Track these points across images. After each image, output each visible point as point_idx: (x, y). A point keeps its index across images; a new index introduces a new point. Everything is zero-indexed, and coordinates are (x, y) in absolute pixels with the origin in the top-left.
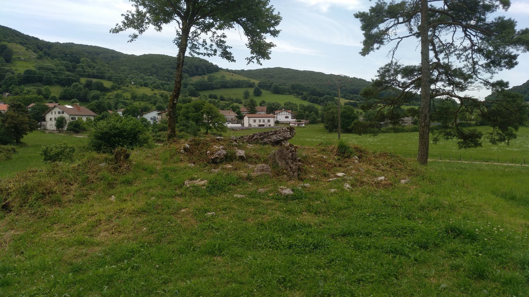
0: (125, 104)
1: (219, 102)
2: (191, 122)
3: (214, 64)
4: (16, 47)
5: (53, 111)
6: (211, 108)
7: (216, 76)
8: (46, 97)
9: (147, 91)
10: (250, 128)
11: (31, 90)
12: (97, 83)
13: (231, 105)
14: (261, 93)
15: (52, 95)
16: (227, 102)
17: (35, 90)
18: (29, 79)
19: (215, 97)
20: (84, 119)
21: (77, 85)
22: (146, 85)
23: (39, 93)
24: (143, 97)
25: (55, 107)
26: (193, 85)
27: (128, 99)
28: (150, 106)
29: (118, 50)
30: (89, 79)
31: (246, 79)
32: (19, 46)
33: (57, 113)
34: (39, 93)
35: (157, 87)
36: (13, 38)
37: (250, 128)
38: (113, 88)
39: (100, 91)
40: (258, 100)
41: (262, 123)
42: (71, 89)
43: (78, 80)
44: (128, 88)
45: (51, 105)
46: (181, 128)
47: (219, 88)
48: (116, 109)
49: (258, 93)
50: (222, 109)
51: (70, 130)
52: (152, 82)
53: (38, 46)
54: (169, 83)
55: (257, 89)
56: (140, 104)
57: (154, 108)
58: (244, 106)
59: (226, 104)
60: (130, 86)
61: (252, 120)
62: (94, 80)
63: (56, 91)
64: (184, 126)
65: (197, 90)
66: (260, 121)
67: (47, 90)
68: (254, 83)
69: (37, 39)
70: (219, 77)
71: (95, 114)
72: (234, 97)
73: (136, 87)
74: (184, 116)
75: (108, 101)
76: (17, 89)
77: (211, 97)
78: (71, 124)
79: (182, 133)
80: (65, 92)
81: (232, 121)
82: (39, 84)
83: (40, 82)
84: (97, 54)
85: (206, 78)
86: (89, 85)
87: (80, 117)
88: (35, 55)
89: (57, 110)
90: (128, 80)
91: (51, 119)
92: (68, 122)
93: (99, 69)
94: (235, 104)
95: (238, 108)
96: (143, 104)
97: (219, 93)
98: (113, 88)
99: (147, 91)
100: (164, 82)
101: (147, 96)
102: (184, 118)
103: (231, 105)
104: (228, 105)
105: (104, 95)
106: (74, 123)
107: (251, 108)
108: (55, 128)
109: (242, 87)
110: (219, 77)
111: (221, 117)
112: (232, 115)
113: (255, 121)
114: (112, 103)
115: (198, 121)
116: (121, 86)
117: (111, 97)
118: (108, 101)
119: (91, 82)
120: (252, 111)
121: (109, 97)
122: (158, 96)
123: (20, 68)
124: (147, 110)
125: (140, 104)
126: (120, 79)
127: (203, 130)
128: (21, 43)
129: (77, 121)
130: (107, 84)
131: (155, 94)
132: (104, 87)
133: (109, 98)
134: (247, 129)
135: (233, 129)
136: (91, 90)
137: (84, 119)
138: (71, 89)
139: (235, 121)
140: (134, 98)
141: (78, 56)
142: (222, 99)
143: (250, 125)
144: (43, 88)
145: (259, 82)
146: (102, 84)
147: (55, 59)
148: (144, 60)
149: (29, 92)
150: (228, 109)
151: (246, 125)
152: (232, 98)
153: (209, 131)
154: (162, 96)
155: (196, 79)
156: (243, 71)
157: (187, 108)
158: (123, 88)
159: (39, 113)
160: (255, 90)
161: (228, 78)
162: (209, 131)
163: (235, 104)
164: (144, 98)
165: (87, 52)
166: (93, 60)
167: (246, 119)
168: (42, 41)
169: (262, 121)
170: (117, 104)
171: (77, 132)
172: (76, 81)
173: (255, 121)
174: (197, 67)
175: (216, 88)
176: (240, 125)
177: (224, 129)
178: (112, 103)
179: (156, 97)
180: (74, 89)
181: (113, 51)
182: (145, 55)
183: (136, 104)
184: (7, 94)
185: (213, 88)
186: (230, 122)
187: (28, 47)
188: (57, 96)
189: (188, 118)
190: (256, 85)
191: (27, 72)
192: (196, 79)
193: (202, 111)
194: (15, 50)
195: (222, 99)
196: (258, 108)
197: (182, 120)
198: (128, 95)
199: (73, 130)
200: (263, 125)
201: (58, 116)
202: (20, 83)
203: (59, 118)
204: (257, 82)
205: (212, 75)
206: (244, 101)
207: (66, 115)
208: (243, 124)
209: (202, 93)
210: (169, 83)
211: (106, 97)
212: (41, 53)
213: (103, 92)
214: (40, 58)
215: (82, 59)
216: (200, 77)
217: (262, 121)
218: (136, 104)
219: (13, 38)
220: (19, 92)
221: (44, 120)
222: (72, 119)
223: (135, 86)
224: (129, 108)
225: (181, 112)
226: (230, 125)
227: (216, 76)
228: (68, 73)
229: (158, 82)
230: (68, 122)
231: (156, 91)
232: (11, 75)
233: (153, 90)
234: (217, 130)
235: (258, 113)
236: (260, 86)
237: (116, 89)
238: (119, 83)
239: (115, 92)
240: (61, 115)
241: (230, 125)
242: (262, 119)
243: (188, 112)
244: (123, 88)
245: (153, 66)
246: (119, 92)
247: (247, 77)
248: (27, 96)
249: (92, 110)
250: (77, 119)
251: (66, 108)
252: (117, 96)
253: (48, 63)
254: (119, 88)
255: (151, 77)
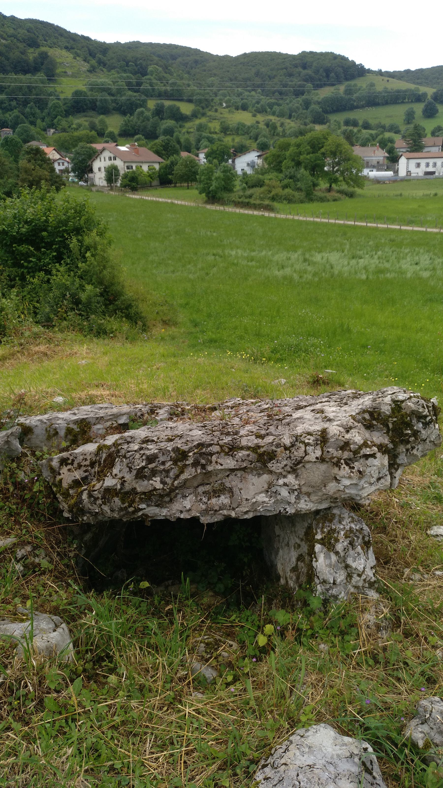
0: (211, 141)
1: (359, 131)
2: (302, 170)
3: (357, 63)
4: (61, 55)
5: (102, 156)
6: (338, 146)
7: (359, 85)
8: (101, 134)
9: (245, 118)
10: (408, 179)
11: (81, 122)
12: (171, 108)
13: (380, 137)
14: (437, 111)
15: (110, 129)
16: (373, 132)
17: (87, 124)
18: (79, 105)
19: (355, 124)
20: (145, 168)
21: (142, 113)
22: (244, 108)
23: (93, 127)
24: (238, 129)
25: (104, 149)
26: (319, 103)
27: (216, 133)
28: (248, 142)
29: (204, 48)
30: (159, 102)
31: (412, 86)
32: (64, 53)
33: (107, 159)
34: (93, 127)
35: (262, 111)
36: (55, 40)
37: (409, 178)
38: (195, 115)
39: (177, 120)
40: (429, 125)
41: (431, 169)
42: (134, 119)
43: (143, 104)
44: (217, 114)
45: (98, 146)
46: (286, 181)
47: (363, 107)
48: (198, 149)
49: (430, 113)
50: (364, 145)
51: (125, 187)
52: (254, 101)
53: (89, 50)
54: (281, 102)
55: (430, 104)
56: (233, 140)
57: (255, 145)
58: (404, 137)
59: (371, 135)
60: (220, 110)
61: (413, 163)
62: (167, 103)
63: (114, 123)
64: (290, 178)
65: (326, 112)
66: (428, 165)
67: (102, 122)
68: (425, 94)
69: (88, 39)
70: (364, 86)
71: (160, 160)
72: (387, 122)
73: (230, 111)
74: (293, 160)
75: (187, 136)
76: (64, 123)
77: (347, 123)
78: (125, 176)
79: (287, 191)
80: (126, 125)
81: (378, 167)
82: (91, 113)
83: (94, 110)
84: (174, 58)
85: (342, 88)
86: (159, 112)
87: (139, 164)
88: (85, 66)
89: (106, 154)
90: (217, 99)
91: (100, 169)
92: (122, 172)
93: (174, 84)
94: (387, 135)
95: (392, 141)
96: (238, 139)
97: (359, 115)
98: (195, 115)
99: (245, 118)
100: (273, 101)
101: (244, 125)
102: (293, 163)
103: (380, 137)
104: (373, 137)
105: (180, 127)
106: (130, 175)
107: (415, 141)
108: (105, 183)
109: (403, 102)
110: (364, 86)
111: (355, 161)
112: (380, 155)
113: (418, 165)
114: (192, 139)
115: (315, 169)
116: (206, 110)
117: (192, 130)
118: (187, 136)
119: (163, 106)
120: (416, 146)
121: (187, 132)
122: (262, 126)
123: (68, 87)
124: (242, 150)
125: (233, 140)
126: (206, 100)
127: (323, 185)
128: (66, 48)
129: (134, 172)
130: (186, 109)
131: (258, 122)
132: (182, 115)
133: (188, 133)
134: (403, 180)
135: (377, 181)
136: (162, 119)
137: (145, 168)
138: (134, 119)
139: (383, 165)
140: (225, 130)
141: (144, 64)
142: (366, 126)
143: (409, 172)
144: (98, 119)
145: (435, 90)
146: (178, 109)
147: (113, 71)
148: (243, 64)
149: (79, 126)
150: (372, 145)
151: (402, 173)
152: (383, 123)
153: (334, 185)
154: (267, 125)
155: (326, 93)
156: (408, 72)
157: (298, 146)
158: (209, 113)
159: (84, 160)
160: (426, 106)
161: (380, 86)
162: (334, 185)
163: (387, 135)
164: (240, 129)
165: (159, 56)
166: (166, 68)
167: (403, 161)
168: (95, 42)
169: (431, 164)
170: (199, 141)
171: (134, 189)
172: (141, 106)
173: (418, 165)
174: (328, 71)
175: (357, 107)
176: (390, 173)
177: (359, 181)
178: (192, 139)
179: (258, 128)
180: (138, 118)
181: (197, 52)
182: (245, 54)
183: (228, 140)
184: (52, 131)
185: (352, 108)
186: (374, 167)
187: (76, 53)
188: (116, 132)
189: (298, 164)
190: (429, 97)
191: (77, 93)
192: (326, 93)
193: (323, 150)
194: (58, 60)
195: (366, 126)
196: (428, 140)
197: (289, 168)
198: (215, 126)
199: (129, 185)
200: (433, 173)
201: (108, 163)
202: (67, 113)
203: (109, 167)
204: (430, 91)
205: (352, 83)
206: (403, 128)
207: (119, 163)
208: (396, 172)
209: (333, 118)
210: (281, 102)
211: (184, 130)
212: (93, 62)
213: (180, 123)
214: (92, 70)
215: (150, 69)
216: (332, 89)
217: (431, 164)
218: (228, 140)
219: (55, 40)
220: (66, 127)
221: (91, 171)
222: (128, 168)
223: (227, 110)
224: (215, 148)
225: (288, 153)
226: (374, 174)
227: (359, 85)
228: (130, 93)
229: (265, 100)
230: (122, 172)
231: (260, 118)
232: (56, 101)
233: (254, 116)
234: (348, 183)
235: (426, 149)
236: (437, 98)
237: (199, 116)
238: (204, 105)
239: (197, 122)
240: (113, 162)
241: (374, 174)
242: (431, 161)
243: (300, 153)
244: (209, 113)
245: (257, 74)
246: (203, 120)
247: (414, 83)
248: (76, 134)
249: (158, 153)
250: (134, 168)
251: (119, 150)
252: (200, 128)
253: (103, 78)
254: (204, 115)
255: (253, 93)
